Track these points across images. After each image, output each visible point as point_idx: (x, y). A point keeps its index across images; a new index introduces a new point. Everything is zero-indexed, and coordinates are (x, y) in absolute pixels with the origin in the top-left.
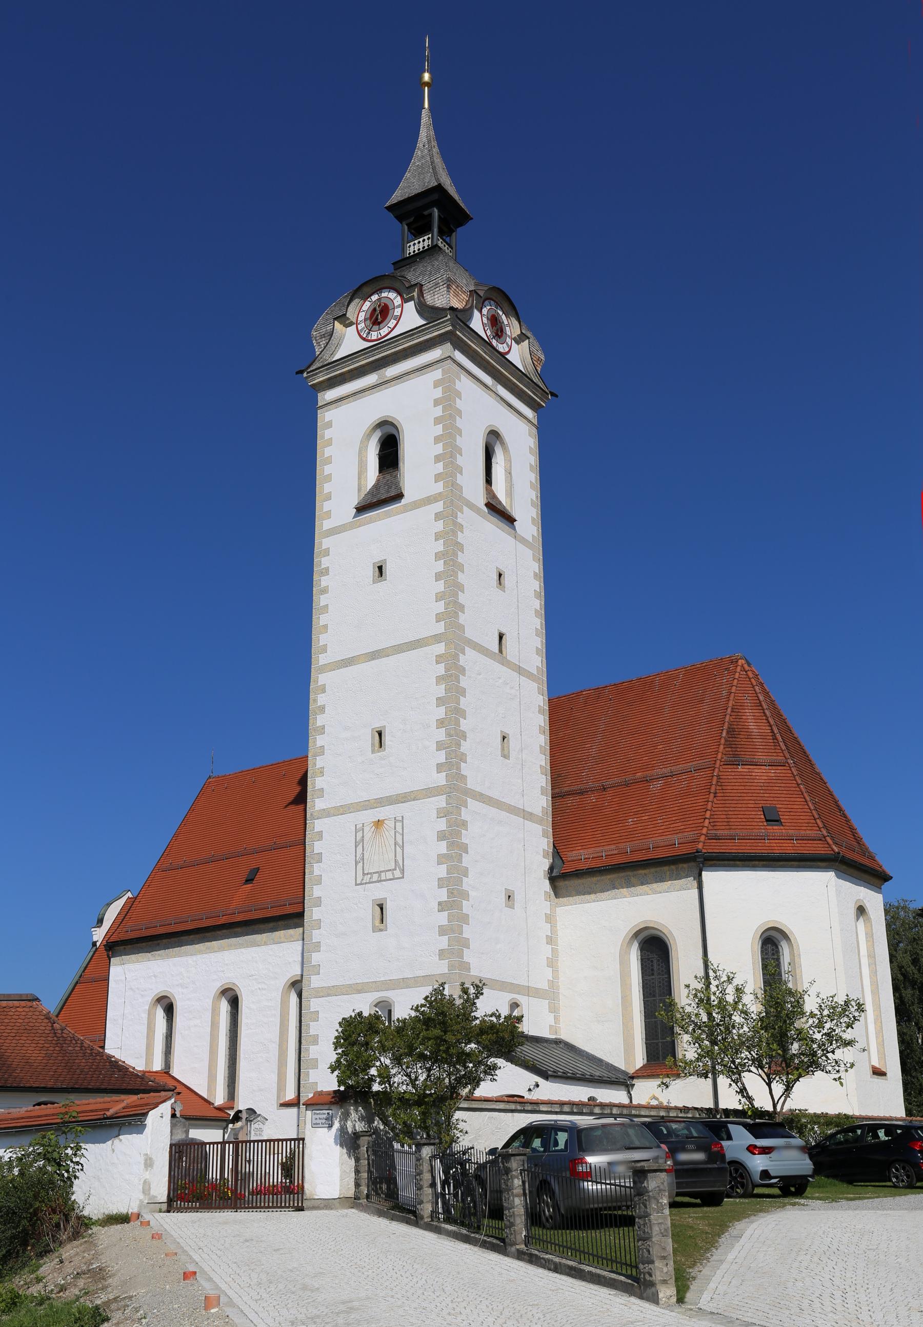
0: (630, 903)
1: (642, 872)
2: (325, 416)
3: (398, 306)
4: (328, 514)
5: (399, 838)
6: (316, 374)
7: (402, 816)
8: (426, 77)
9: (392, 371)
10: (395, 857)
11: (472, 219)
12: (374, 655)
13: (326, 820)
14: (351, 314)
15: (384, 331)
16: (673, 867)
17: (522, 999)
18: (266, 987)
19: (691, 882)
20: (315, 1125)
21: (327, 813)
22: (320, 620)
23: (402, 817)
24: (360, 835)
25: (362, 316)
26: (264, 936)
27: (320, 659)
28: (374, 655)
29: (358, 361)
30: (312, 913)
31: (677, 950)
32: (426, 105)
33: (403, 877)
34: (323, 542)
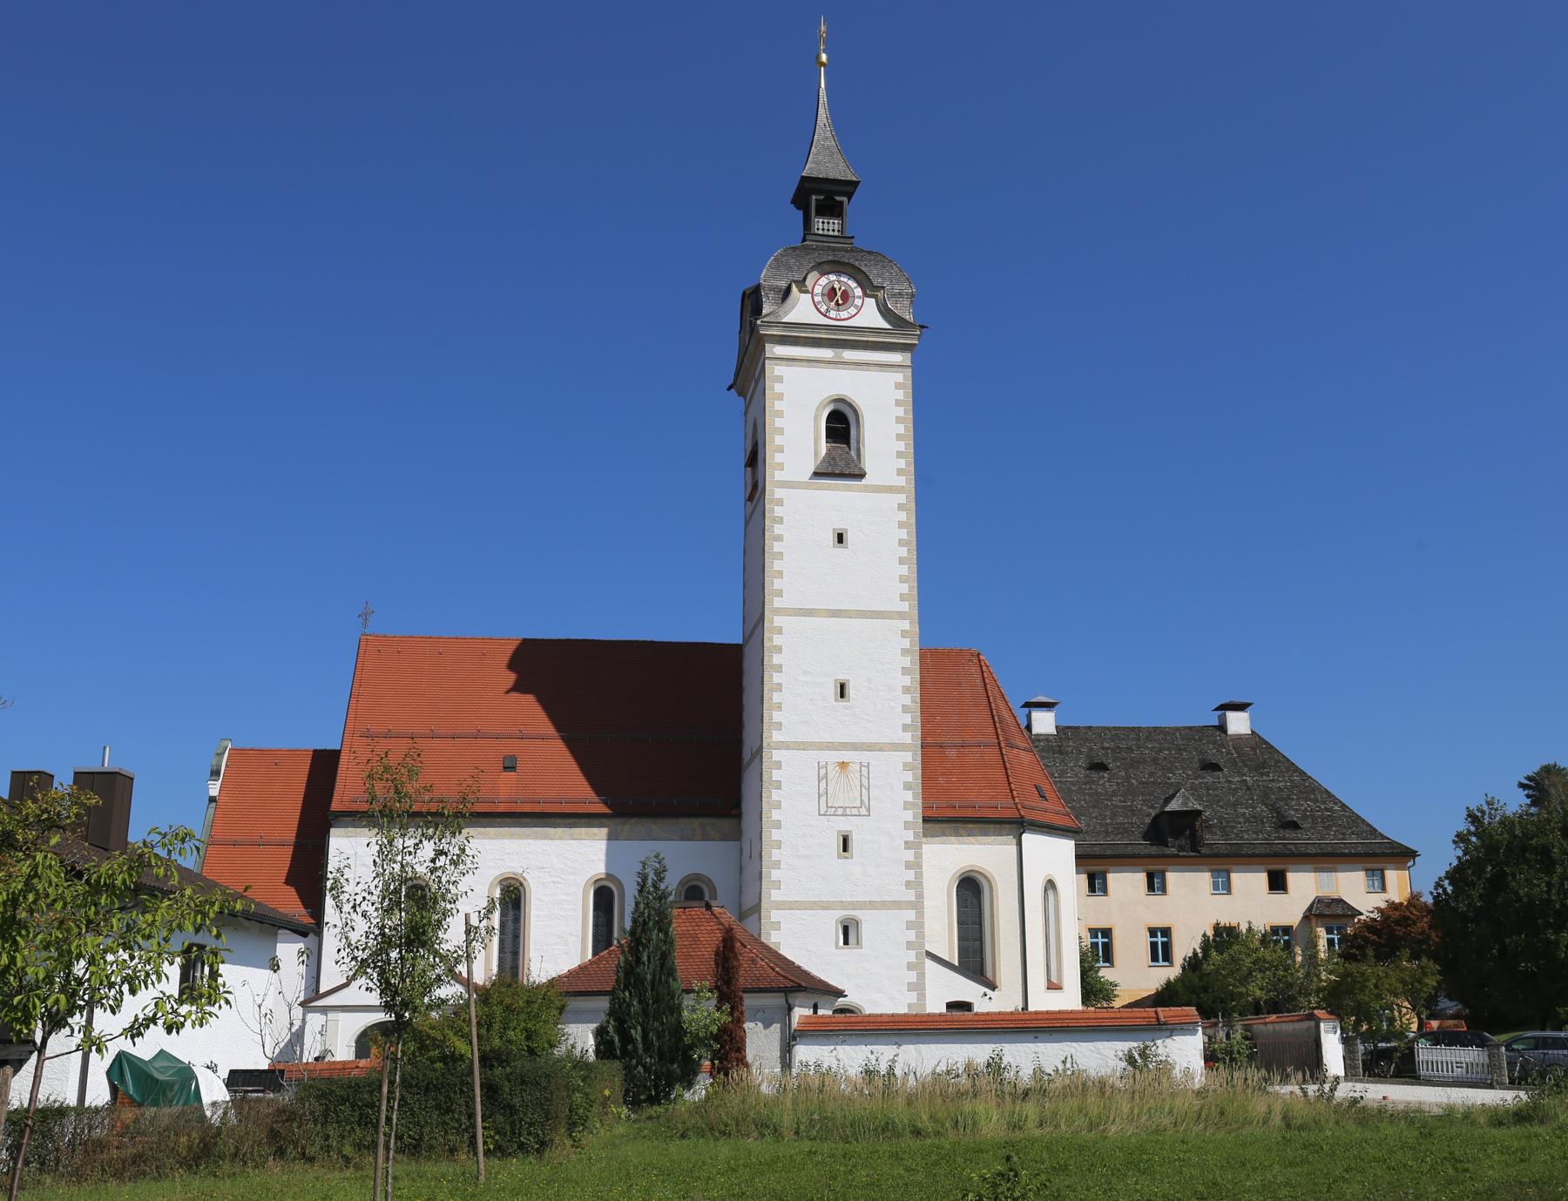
0: (957, 849)
1: (971, 826)
2: (773, 370)
3: (859, 297)
5: (865, 781)
6: (771, 326)
7: (868, 763)
8: (824, 57)
9: (849, 355)
10: (861, 796)
12: (836, 613)
13: (784, 752)
14: (809, 283)
15: (844, 314)
16: (998, 826)
18: (562, 881)
19: (1011, 839)
20: (1327, 1032)
23: (868, 763)
24: (823, 772)
25: (818, 290)
26: (559, 830)
28: (836, 613)
29: (819, 333)
31: (997, 891)
32: (823, 85)
33: (869, 815)
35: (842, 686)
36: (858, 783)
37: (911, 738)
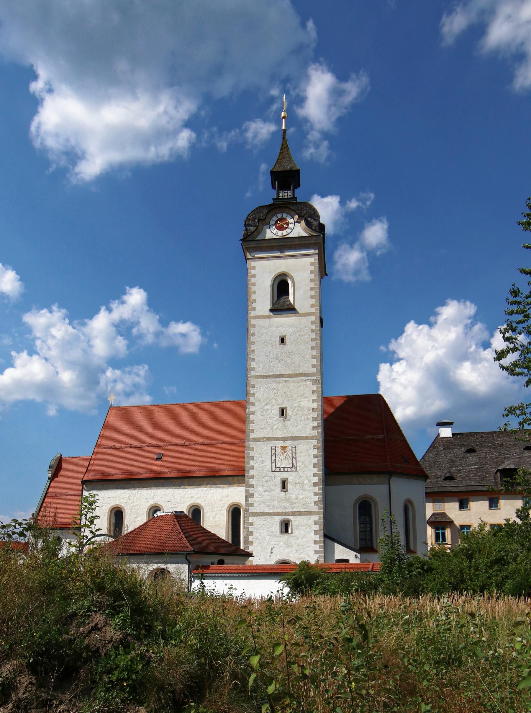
4: (254, 309)
5: (294, 455)
24: (274, 451)
36: (291, 456)
37: (318, 433)
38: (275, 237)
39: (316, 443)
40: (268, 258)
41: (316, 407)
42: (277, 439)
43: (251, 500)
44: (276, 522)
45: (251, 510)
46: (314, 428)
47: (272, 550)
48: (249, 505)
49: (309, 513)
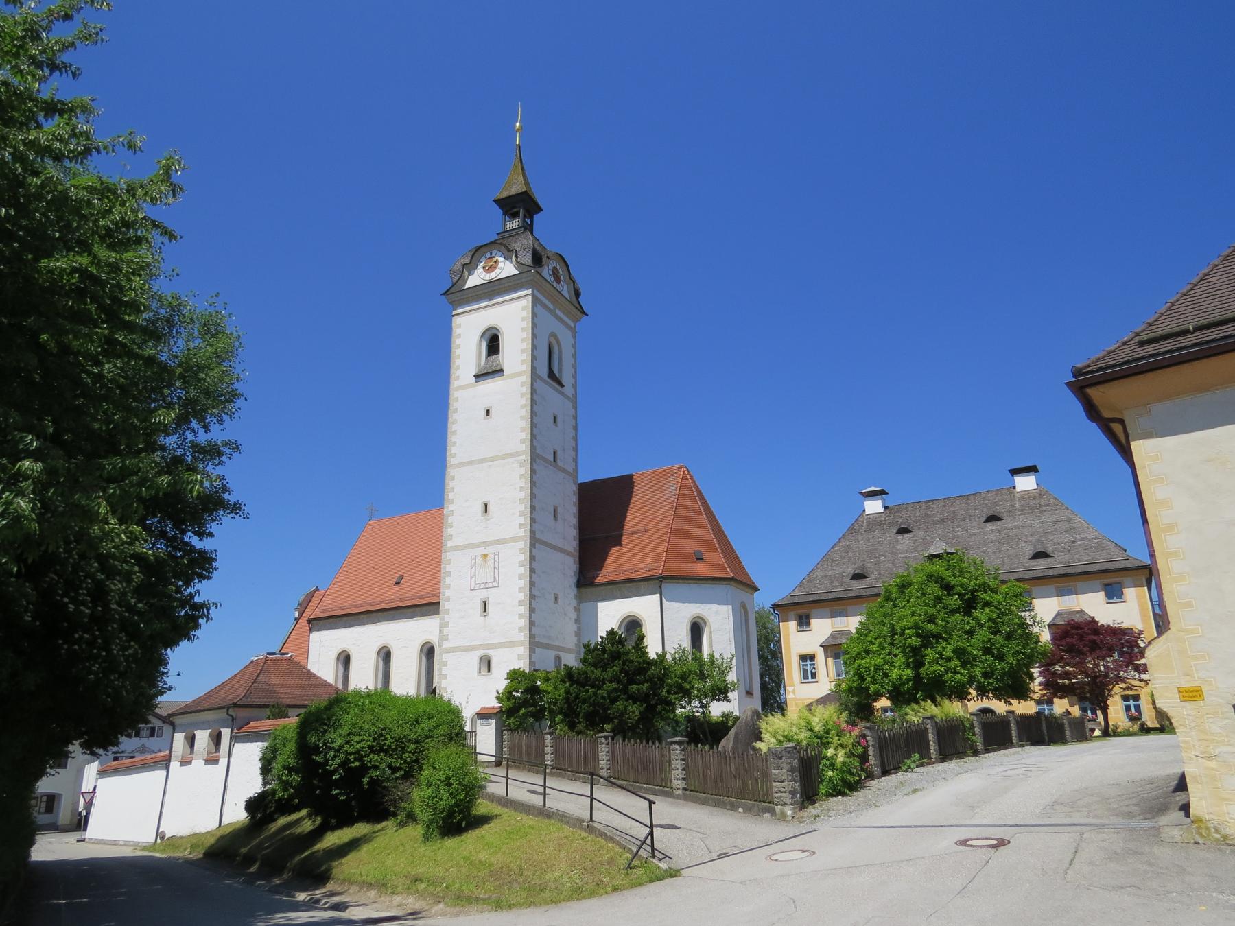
4: (458, 378)
11: (542, 210)
17: (561, 654)
21: (455, 549)
22: (452, 438)
24: (474, 561)
27: (451, 461)
30: (444, 606)
34: (455, 394)
35: (486, 505)
36: (492, 566)
37: (524, 533)
38: (483, 282)
39: (523, 546)
40: (475, 310)
41: (524, 497)
42: (478, 545)
43: (446, 630)
44: (473, 658)
45: (446, 645)
46: (521, 525)
47: (468, 698)
48: (443, 638)
49: (512, 644)
